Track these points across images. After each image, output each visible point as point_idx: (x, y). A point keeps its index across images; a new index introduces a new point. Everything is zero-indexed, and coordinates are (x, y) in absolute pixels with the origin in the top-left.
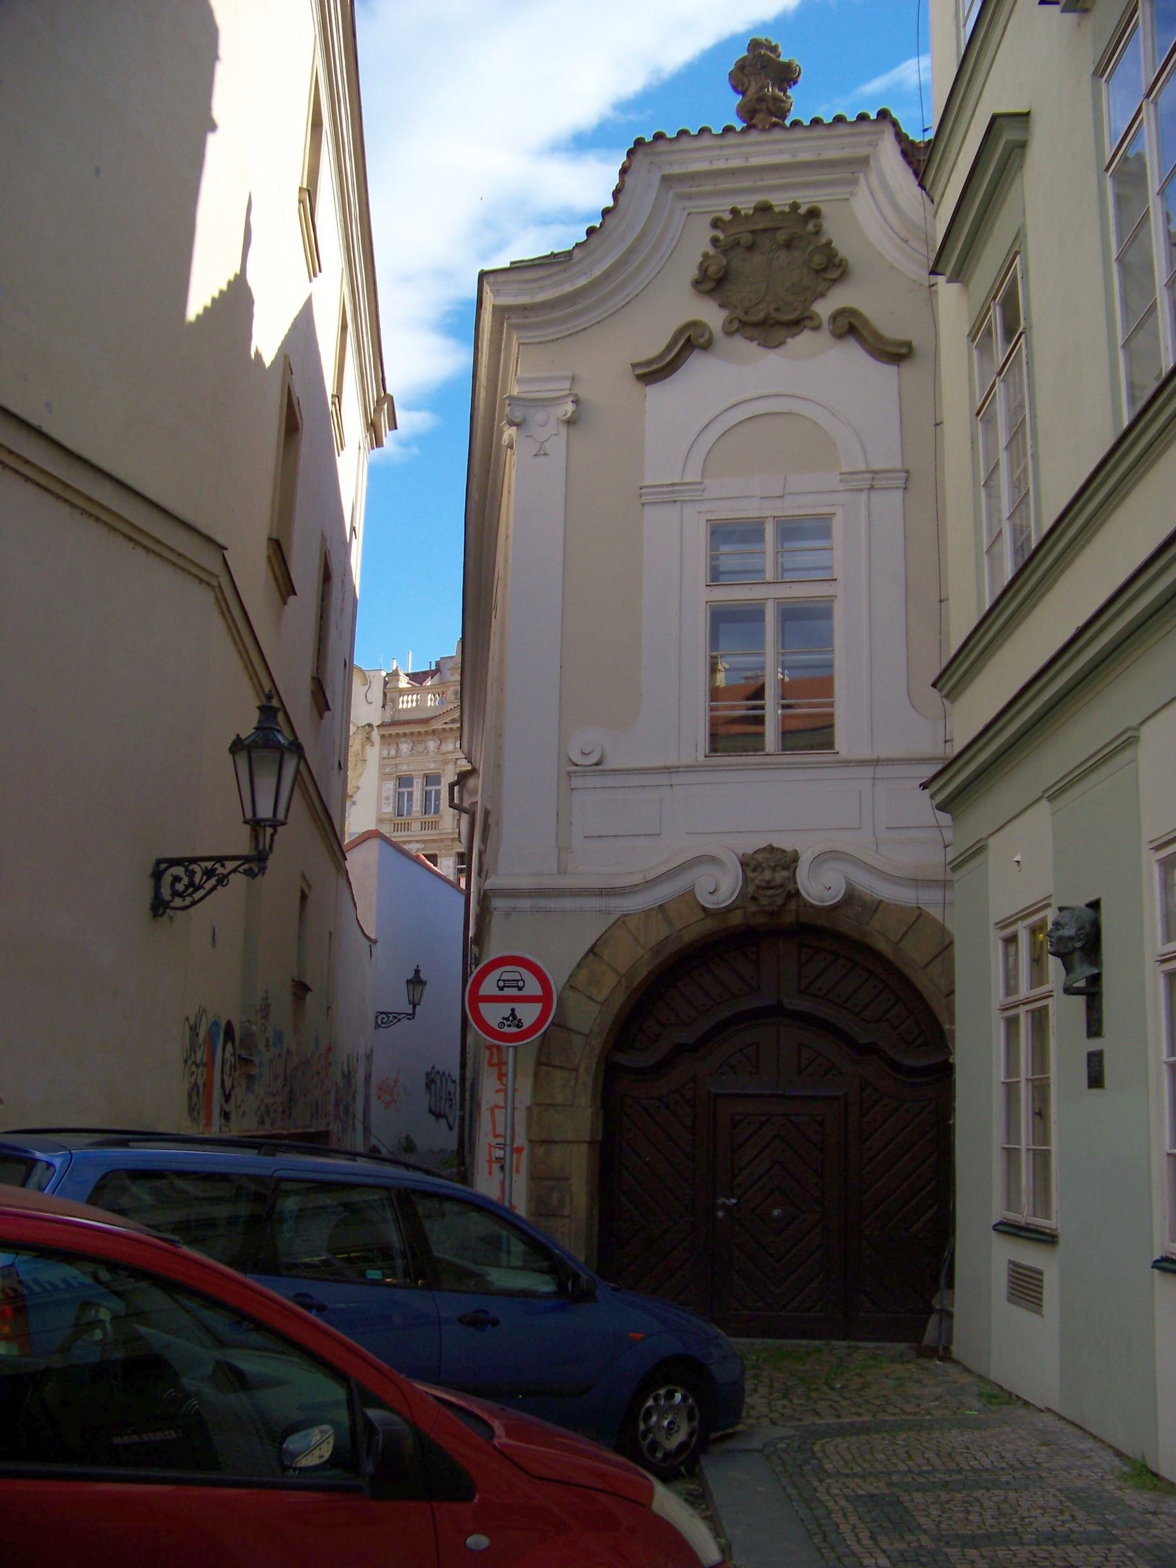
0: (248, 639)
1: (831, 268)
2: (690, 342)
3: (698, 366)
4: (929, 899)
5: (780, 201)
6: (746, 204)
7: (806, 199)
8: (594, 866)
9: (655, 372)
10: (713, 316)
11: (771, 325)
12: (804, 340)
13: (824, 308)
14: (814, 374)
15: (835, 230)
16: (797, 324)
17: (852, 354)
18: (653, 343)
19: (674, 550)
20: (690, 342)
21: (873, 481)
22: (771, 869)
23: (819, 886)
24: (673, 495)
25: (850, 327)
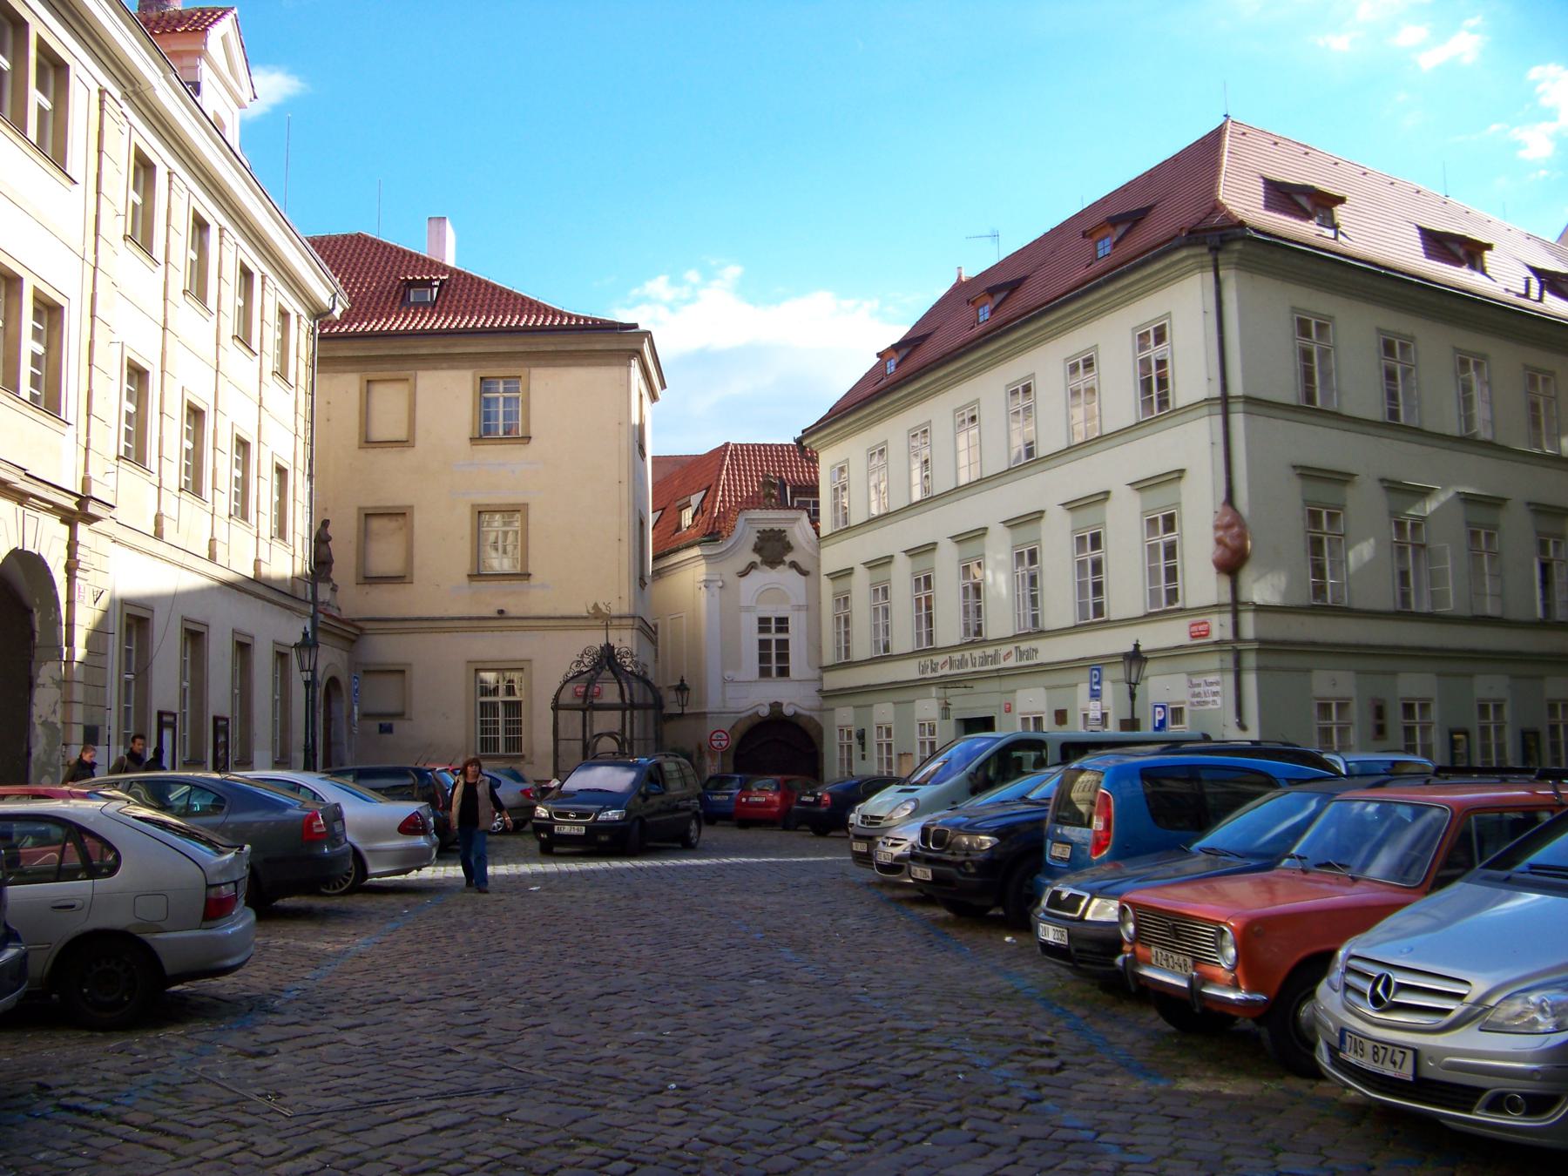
0: (552, 623)
1: (788, 547)
2: (752, 566)
3: (753, 572)
4: (815, 715)
5: (776, 527)
6: (767, 527)
7: (782, 526)
8: (732, 705)
9: (743, 574)
10: (757, 558)
11: (773, 561)
12: (781, 567)
13: (788, 559)
14: (782, 576)
15: (790, 538)
16: (782, 562)
17: (794, 572)
18: (742, 567)
19: (750, 626)
20: (752, 566)
21: (799, 608)
22: (776, 706)
23: (788, 711)
24: (748, 609)
25: (794, 565)
